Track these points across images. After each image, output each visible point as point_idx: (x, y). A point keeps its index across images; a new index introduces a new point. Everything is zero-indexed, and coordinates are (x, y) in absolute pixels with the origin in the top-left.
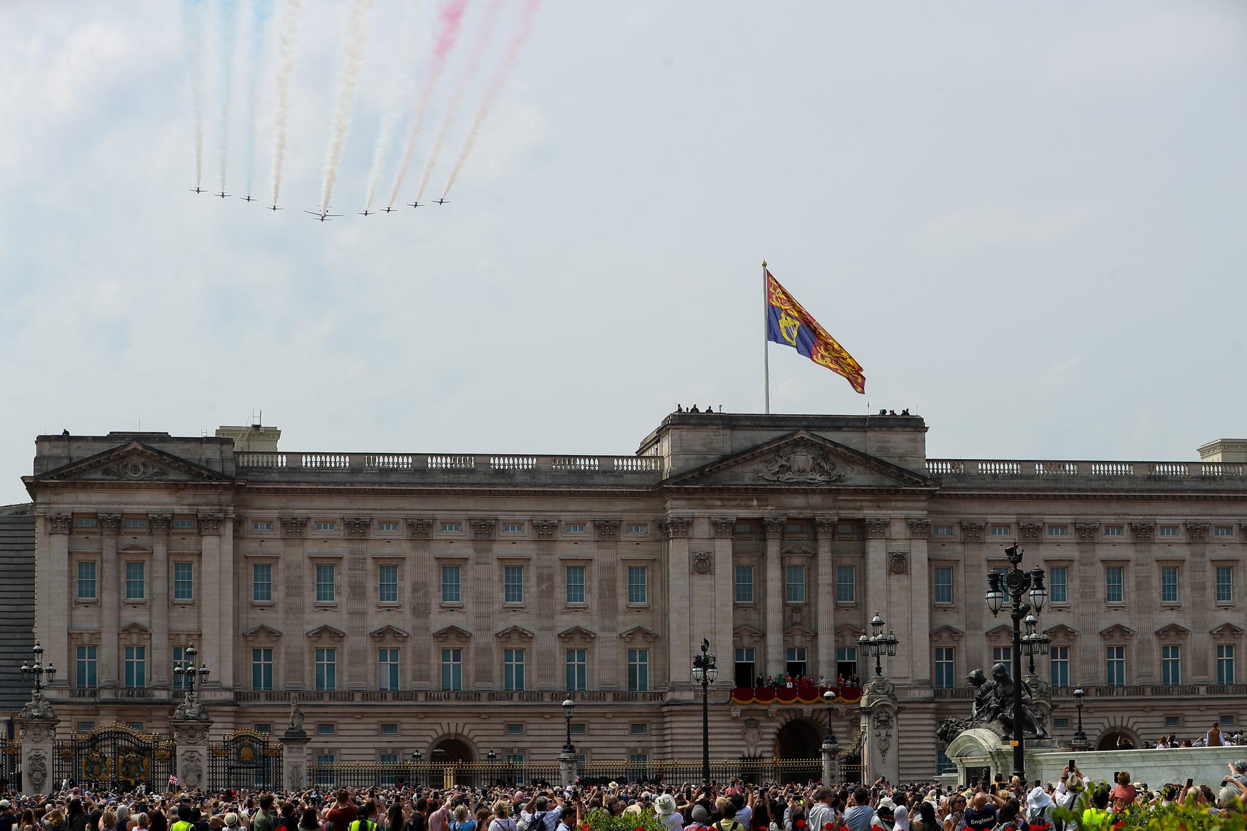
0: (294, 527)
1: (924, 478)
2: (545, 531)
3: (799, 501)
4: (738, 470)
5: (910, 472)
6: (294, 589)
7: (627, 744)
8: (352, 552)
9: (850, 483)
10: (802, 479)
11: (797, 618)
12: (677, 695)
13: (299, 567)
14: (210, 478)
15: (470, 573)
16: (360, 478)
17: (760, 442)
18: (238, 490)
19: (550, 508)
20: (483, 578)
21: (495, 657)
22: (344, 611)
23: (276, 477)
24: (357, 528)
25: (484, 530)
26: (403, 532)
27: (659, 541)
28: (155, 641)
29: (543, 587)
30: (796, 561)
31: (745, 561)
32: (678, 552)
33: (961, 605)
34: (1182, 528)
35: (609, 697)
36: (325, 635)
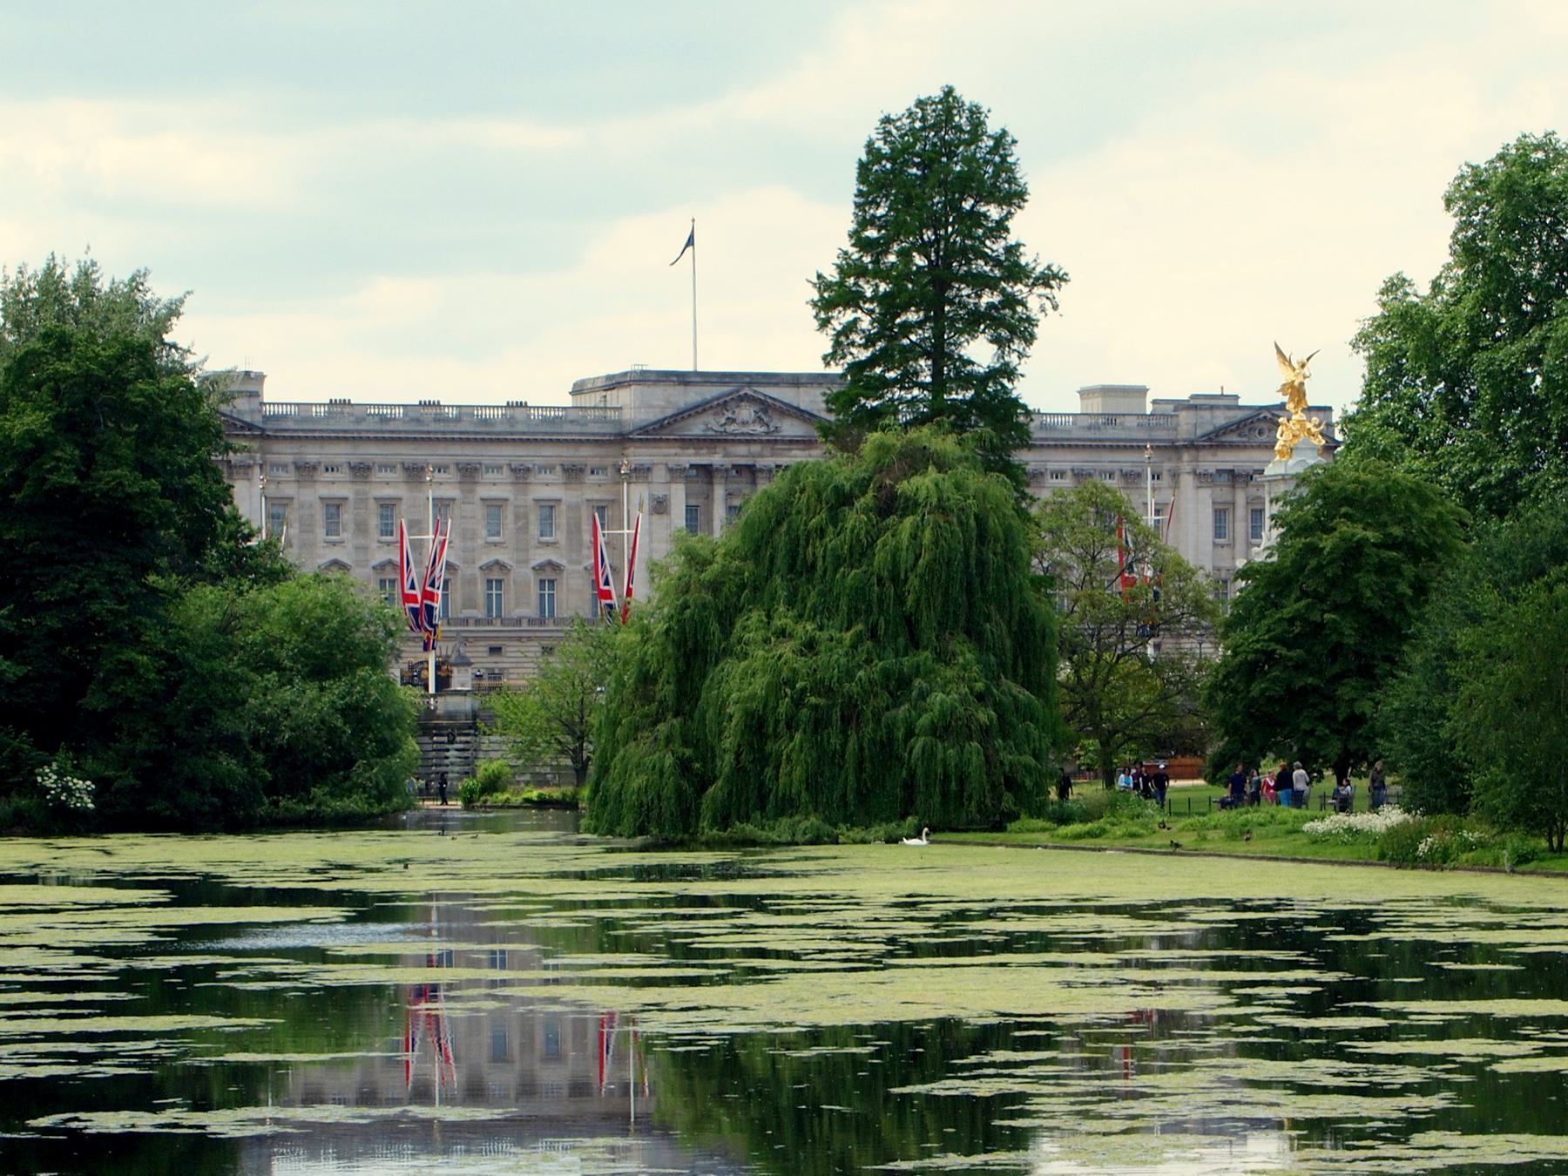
0: (306, 471)
2: (521, 474)
3: (742, 449)
4: (691, 421)
6: (307, 527)
8: (357, 493)
10: (745, 430)
16: (363, 427)
17: (708, 397)
22: (350, 545)
23: (291, 425)
24: (361, 471)
25: (469, 473)
26: (399, 475)
31: (692, 502)
34: (1069, 473)
36: (334, 569)
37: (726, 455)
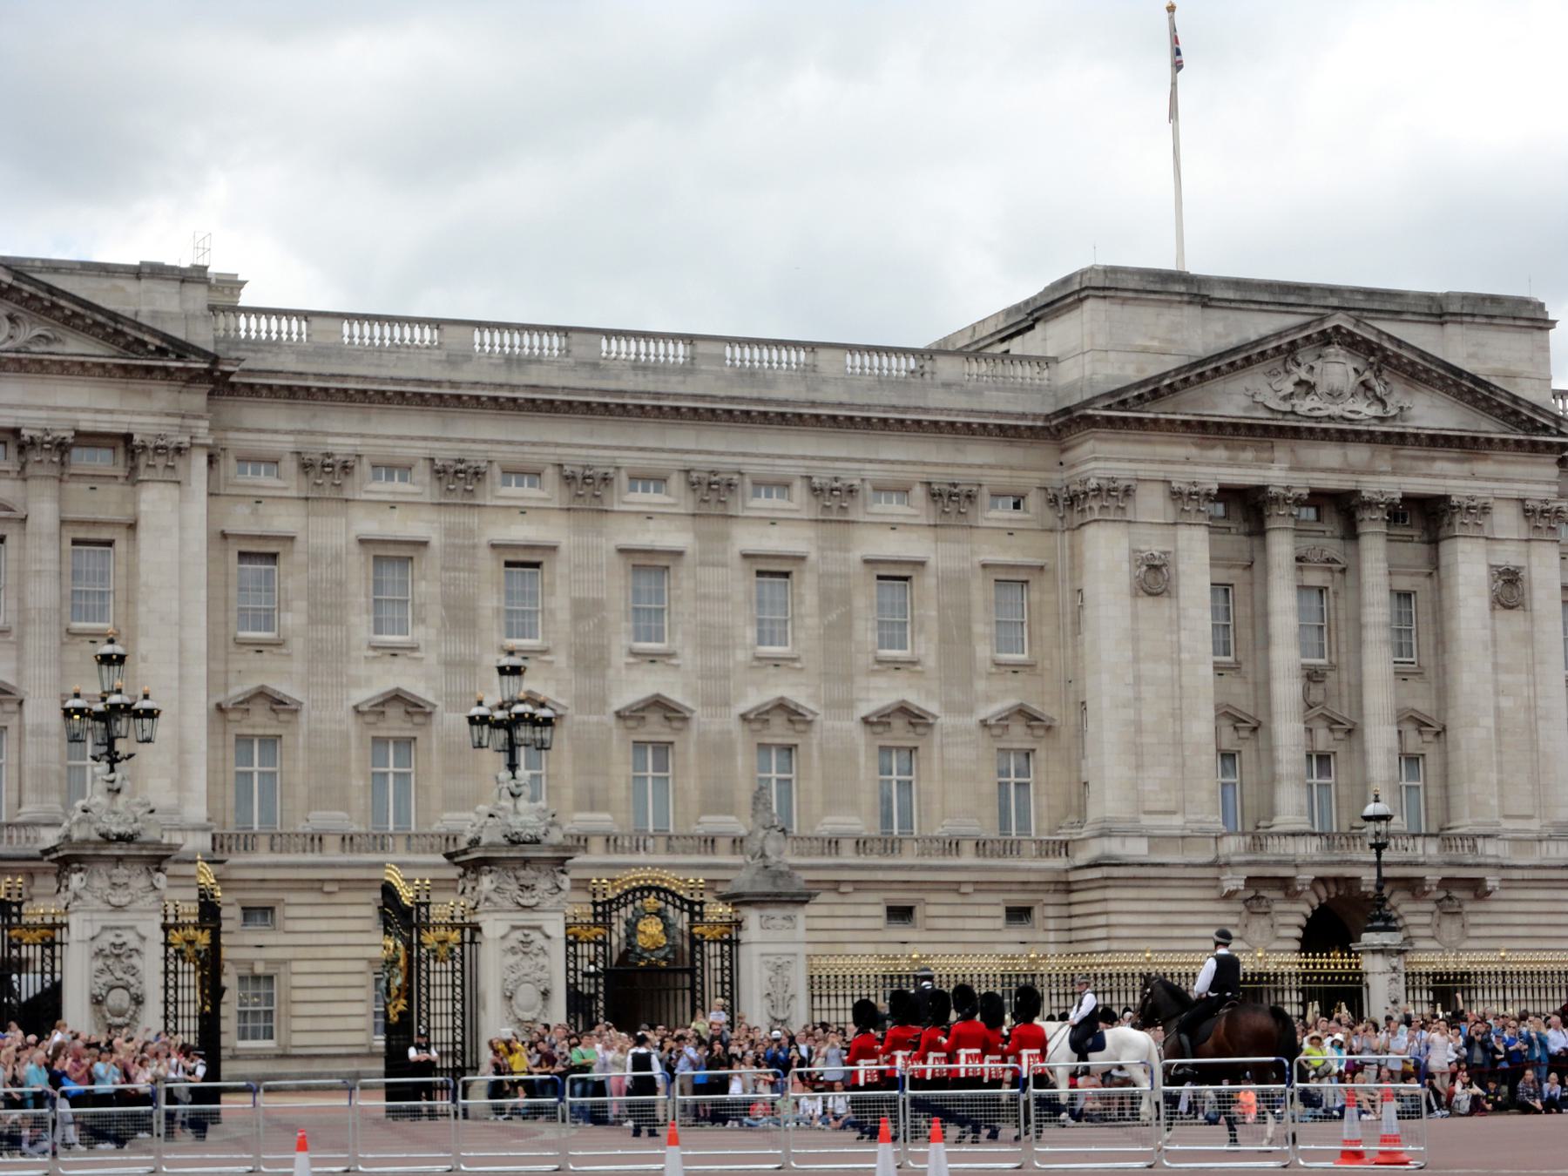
0: (326, 473)
2: (834, 499)
3: (1329, 455)
4: (1217, 385)
5: (1535, 408)
6: (327, 607)
7: (1000, 949)
8: (449, 532)
9: (1418, 424)
10: (1335, 410)
11: (1317, 693)
12: (1114, 847)
13: (337, 558)
14: (161, 352)
15: (687, 584)
16: (466, 374)
19: (844, 454)
20: (713, 590)
22: (431, 658)
23: (289, 363)
24: (459, 479)
25: (713, 492)
26: (549, 492)
27: (1051, 531)
28: (30, 714)
29: (833, 616)
30: (1315, 578)
31: (1223, 576)
32: (1107, 551)
35: (968, 846)
36: (395, 712)
37: (1296, 468)
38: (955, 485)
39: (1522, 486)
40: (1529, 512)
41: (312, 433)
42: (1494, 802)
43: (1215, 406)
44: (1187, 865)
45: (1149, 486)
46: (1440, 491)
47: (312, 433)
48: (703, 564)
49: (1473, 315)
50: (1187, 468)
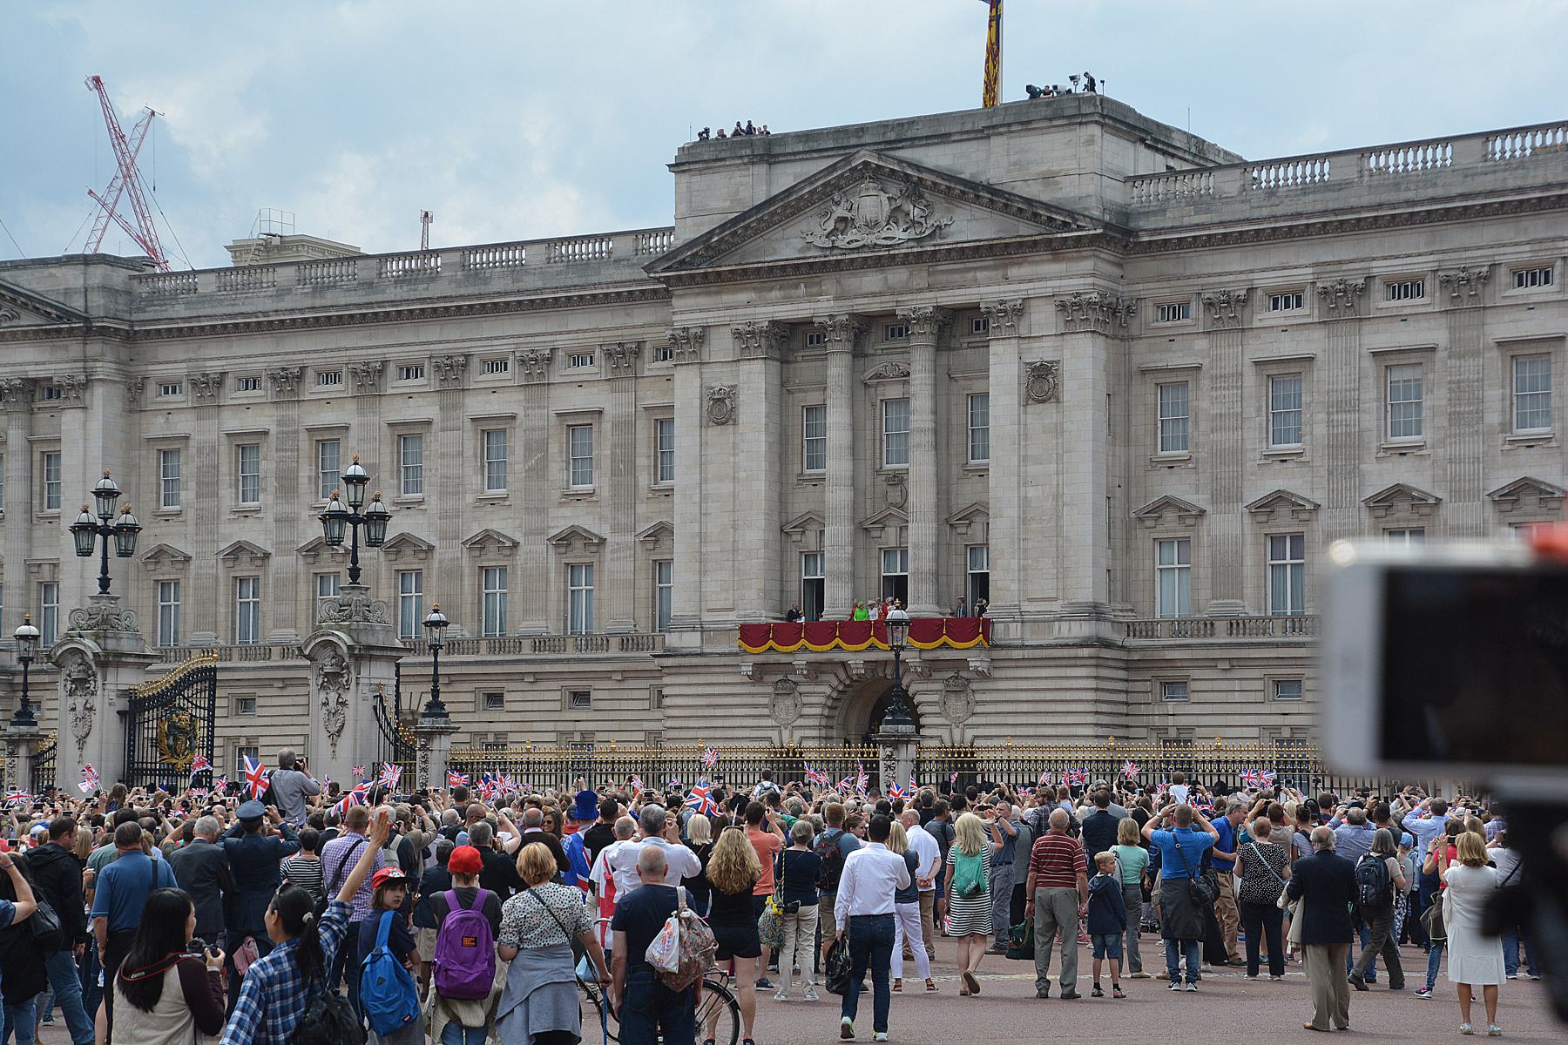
1: (1071, 213)
3: (871, 281)
4: (776, 234)
6: (208, 487)
7: (647, 726)
8: (280, 423)
10: (871, 239)
11: (895, 495)
13: (214, 450)
15: (434, 446)
16: (287, 303)
18: (130, 337)
20: (450, 452)
21: (467, 582)
22: (269, 517)
33: (1203, 454)
35: (614, 642)
38: (620, 344)
39: (1057, 283)
40: (1071, 309)
41: (197, 360)
42: (1014, 587)
43: (775, 252)
44: (720, 655)
45: (722, 330)
46: (974, 299)
47: (197, 360)
48: (443, 430)
49: (1009, 125)
50: (748, 311)
